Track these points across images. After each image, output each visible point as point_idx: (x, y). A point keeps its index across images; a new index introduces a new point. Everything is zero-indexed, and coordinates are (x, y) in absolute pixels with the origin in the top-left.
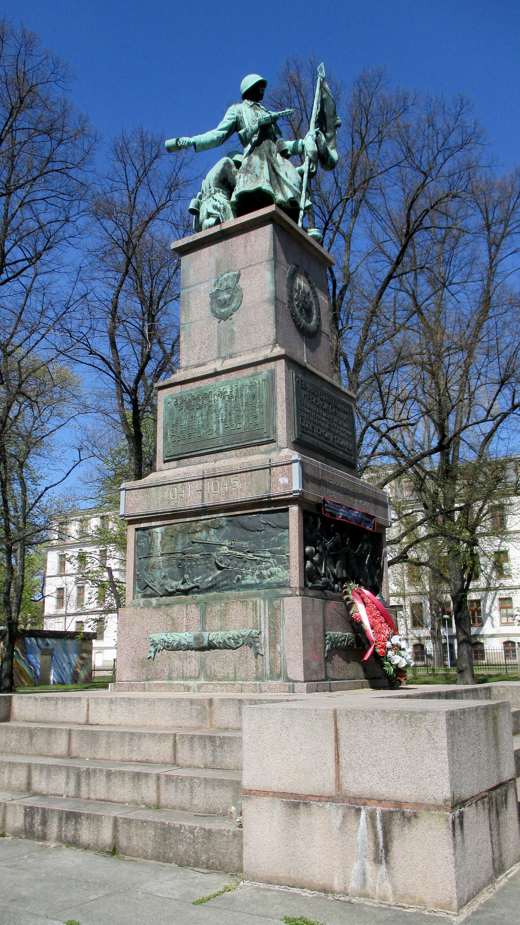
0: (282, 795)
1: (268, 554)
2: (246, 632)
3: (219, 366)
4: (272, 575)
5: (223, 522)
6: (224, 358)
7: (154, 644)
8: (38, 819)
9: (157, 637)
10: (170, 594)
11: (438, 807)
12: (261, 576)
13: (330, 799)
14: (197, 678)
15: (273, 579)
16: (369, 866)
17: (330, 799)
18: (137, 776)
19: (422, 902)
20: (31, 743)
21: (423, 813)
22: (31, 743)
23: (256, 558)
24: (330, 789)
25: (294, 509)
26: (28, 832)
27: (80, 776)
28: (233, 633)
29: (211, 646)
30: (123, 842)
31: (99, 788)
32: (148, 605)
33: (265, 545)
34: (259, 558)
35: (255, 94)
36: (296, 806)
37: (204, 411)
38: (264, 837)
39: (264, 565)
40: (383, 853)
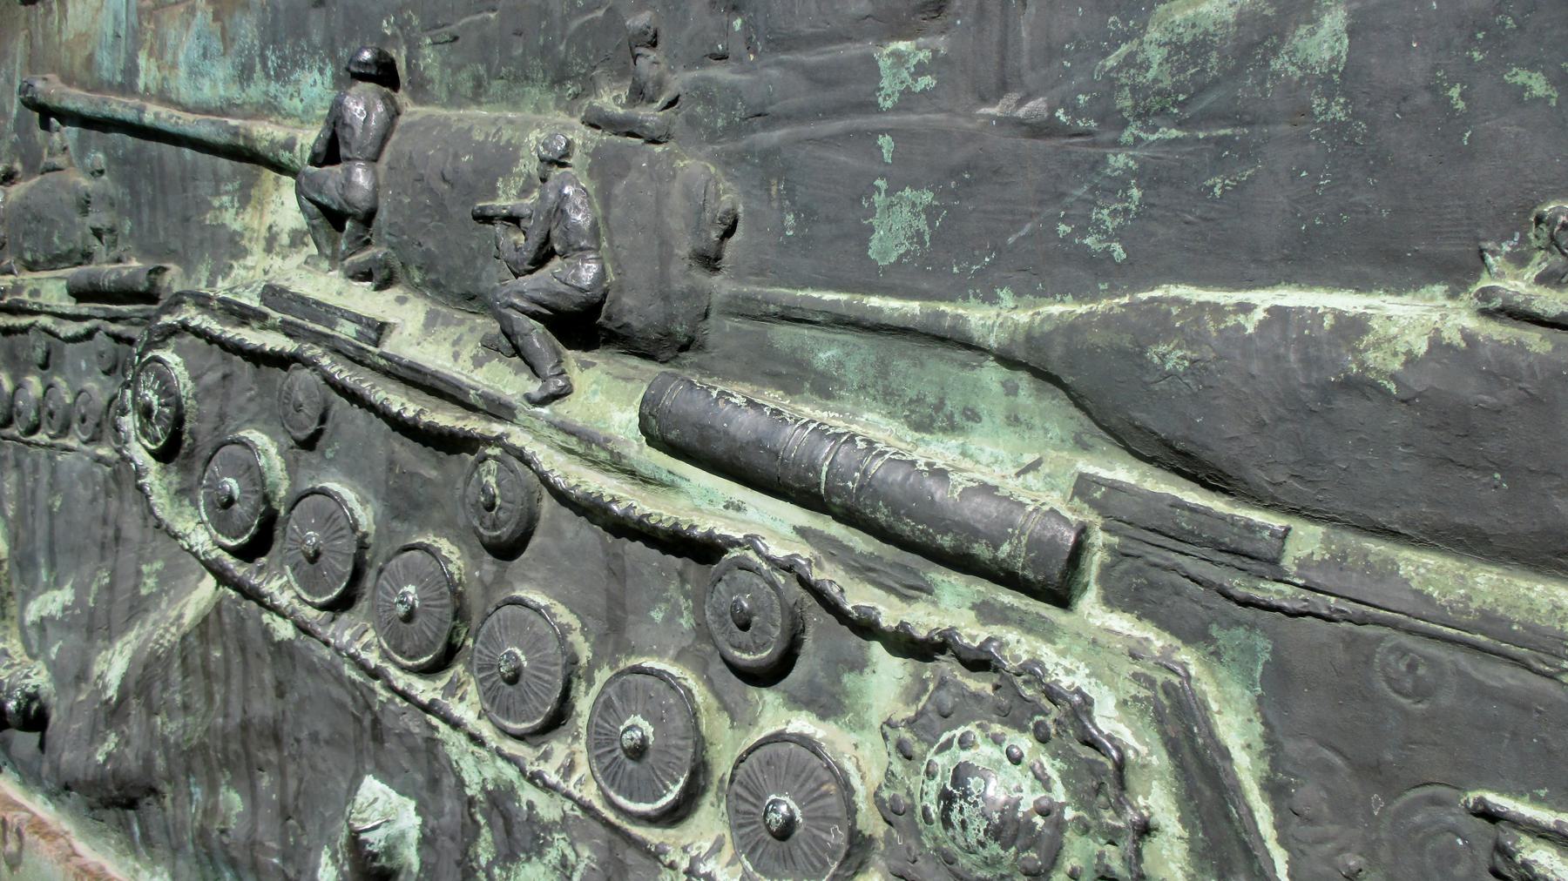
1: (1014, 465)
23: (702, 502)
33: (963, 178)
34: (773, 526)
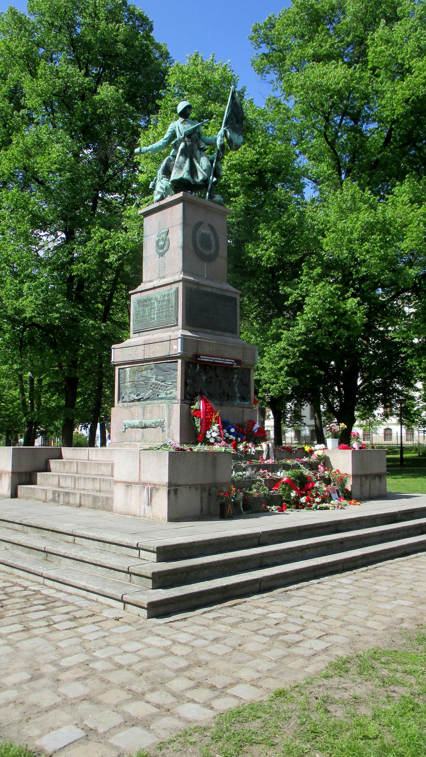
0: (125, 482)
2: (159, 420)
3: (156, 283)
4: (171, 393)
5: (153, 366)
6: (161, 278)
7: (125, 426)
8: (57, 495)
9: (126, 422)
10: (133, 401)
11: (165, 486)
12: (166, 394)
13: (137, 484)
14: (140, 441)
15: (171, 395)
16: (146, 506)
17: (137, 484)
18: (94, 479)
19: (159, 518)
20: (64, 468)
21: (161, 488)
22: (64, 468)
24: (137, 480)
25: (180, 361)
26: (54, 500)
27: (75, 479)
28: (154, 421)
29: (145, 427)
30: (83, 503)
31: (81, 484)
32: (123, 406)
35: (185, 114)
36: (128, 486)
37: (149, 307)
38: (120, 498)
39: (168, 388)
40: (150, 502)
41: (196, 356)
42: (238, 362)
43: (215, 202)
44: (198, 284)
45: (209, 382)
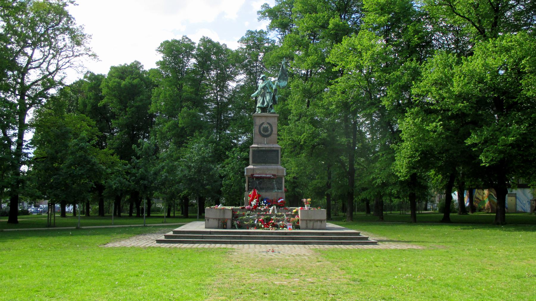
41: (252, 175)
42: (274, 175)
43: (271, 113)
44: (258, 147)
45: (260, 184)
